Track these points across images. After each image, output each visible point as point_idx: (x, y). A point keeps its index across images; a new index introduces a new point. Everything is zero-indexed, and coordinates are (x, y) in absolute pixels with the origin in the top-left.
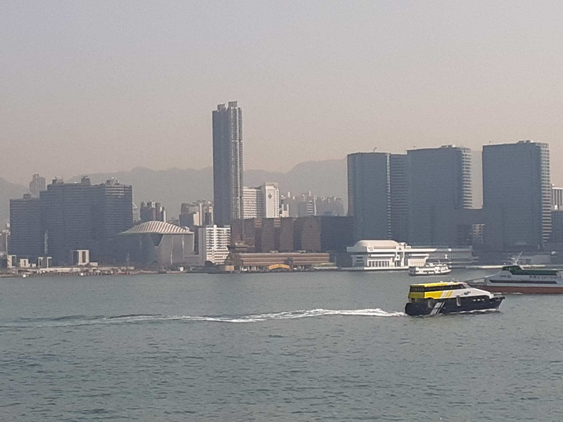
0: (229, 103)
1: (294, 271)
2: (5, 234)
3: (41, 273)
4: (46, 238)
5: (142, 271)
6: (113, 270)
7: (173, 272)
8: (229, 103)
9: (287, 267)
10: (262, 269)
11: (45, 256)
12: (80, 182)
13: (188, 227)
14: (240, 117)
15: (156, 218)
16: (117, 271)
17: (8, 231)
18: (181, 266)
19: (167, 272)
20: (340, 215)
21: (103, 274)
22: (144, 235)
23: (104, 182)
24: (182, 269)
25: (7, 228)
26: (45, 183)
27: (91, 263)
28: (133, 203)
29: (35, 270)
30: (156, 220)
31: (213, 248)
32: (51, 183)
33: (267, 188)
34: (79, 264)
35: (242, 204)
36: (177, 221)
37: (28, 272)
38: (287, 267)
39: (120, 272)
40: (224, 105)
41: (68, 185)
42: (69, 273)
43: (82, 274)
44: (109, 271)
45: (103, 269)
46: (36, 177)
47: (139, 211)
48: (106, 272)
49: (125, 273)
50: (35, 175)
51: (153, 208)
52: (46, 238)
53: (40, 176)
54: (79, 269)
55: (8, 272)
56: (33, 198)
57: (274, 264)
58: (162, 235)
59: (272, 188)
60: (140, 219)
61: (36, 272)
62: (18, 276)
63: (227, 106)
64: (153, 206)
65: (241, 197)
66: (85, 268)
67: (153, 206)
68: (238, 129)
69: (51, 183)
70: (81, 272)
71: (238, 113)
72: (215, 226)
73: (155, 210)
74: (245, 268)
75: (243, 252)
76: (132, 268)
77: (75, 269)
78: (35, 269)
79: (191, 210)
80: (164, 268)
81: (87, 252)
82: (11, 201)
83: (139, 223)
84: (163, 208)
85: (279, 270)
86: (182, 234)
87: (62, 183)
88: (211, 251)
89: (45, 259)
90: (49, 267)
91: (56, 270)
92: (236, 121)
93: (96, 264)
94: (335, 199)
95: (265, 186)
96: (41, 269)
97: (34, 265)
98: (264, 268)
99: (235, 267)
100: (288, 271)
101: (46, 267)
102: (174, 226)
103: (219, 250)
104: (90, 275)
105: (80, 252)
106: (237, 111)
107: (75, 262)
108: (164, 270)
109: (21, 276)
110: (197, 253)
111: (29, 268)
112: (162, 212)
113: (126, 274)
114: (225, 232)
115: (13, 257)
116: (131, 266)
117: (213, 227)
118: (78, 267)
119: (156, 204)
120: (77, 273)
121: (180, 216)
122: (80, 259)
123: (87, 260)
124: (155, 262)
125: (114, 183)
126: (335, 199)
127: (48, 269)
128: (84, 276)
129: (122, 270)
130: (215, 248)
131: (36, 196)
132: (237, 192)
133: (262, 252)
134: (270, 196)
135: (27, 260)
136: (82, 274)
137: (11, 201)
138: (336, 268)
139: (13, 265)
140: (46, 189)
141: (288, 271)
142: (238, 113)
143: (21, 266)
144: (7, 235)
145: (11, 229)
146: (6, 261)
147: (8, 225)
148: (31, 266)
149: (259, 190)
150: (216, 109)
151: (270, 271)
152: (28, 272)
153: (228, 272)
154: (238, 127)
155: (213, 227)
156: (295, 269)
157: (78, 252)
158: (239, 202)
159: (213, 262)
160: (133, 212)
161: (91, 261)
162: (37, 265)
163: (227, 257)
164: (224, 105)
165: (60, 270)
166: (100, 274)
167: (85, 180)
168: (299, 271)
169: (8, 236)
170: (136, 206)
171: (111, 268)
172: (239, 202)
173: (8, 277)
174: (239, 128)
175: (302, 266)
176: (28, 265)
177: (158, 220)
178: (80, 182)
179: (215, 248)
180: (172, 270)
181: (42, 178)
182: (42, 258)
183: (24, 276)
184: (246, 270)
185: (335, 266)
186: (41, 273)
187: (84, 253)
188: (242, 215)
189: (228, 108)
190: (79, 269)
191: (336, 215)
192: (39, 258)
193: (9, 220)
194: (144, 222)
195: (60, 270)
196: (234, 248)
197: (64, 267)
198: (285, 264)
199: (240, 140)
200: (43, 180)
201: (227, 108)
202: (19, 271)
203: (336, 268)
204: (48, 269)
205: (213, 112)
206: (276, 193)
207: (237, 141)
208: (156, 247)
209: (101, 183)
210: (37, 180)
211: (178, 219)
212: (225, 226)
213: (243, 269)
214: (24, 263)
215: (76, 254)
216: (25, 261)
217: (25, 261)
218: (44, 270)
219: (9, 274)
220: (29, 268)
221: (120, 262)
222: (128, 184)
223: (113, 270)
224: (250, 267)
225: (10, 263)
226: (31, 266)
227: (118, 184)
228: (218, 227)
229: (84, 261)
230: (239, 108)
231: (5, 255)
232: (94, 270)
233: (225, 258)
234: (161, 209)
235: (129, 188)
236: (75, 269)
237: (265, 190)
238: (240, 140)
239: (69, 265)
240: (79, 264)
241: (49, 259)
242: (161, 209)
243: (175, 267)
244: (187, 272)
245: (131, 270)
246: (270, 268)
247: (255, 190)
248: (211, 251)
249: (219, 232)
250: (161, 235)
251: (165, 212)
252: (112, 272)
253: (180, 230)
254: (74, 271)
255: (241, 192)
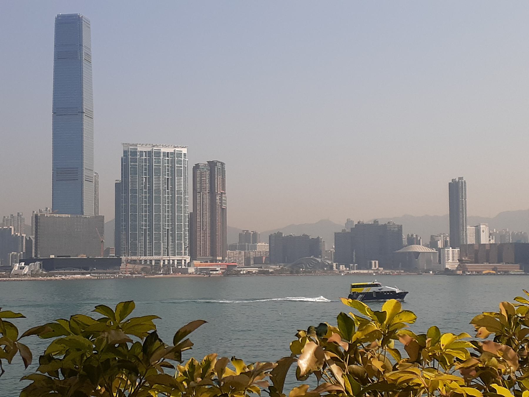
0: (459, 178)
1: (498, 275)
2: (332, 252)
3: (351, 273)
4: (354, 254)
5: (408, 273)
6: (392, 272)
7: (426, 274)
8: (459, 178)
9: (494, 272)
10: (479, 273)
11: (354, 264)
12: (373, 223)
13: (435, 248)
14: (465, 186)
15: (416, 243)
16: (394, 273)
17: (333, 249)
18: (431, 271)
19: (423, 274)
20: (526, 242)
21: (386, 274)
22: (410, 253)
23: (387, 223)
24: (431, 272)
25: (333, 248)
26: (353, 224)
27: (379, 268)
28: (403, 235)
29: (348, 272)
30: (416, 244)
31: (449, 260)
32: (357, 223)
33: (481, 226)
34: (373, 268)
35: (466, 236)
36: (428, 245)
37: (345, 272)
38: (494, 272)
39: (396, 273)
40: (456, 179)
41: (366, 225)
42: (368, 274)
43: (374, 274)
44: (390, 273)
45: (386, 271)
46: (349, 220)
47: (406, 239)
48: (388, 273)
49: (399, 274)
50: (348, 219)
51: (414, 238)
52: (354, 254)
53: (351, 220)
54: (372, 272)
55: (334, 272)
56: (347, 232)
57: (486, 270)
58: (420, 253)
59: (484, 226)
60: (407, 243)
61: (349, 273)
62: (339, 275)
63: (457, 180)
64: (414, 236)
65: (466, 231)
66: (376, 271)
67: (414, 236)
68: (464, 193)
69: (357, 223)
70: (374, 273)
71: (464, 184)
72: (451, 248)
73: (415, 239)
74: (468, 272)
75: (467, 263)
76: (403, 271)
77: (370, 271)
78: (348, 271)
79: (436, 239)
80: (421, 272)
81: (377, 262)
82: (335, 233)
83: (406, 246)
84: (420, 238)
85: (489, 274)
86: (431, 252)
87: (363, 223)
88: (448, 262)
89: (354, 266)
90: (356, 270)
91: (360, 272)
92: (463, 189)
93: (382, 269)
94: (523, 233)
95: (480, 225)
96: (352, 271)
97: (348, 269)
98: (480, 273)
99: (463, 272)
100: (494, 274)
101: (354, 270)
102: (424, 247)
103: (453, 262)
104: (379, 274)
105: (373, 262)
106: (463, 182)
107: (370, 268)
108: (421, 273)
109: (341, 275)
110: (440, 263)
111: (345, 270)
112: (420, 240)
113: (399, 274)
114: (457, 251)
115: (336, 264)
116: (402, 270)
117: (449, 248)
118: (372, 270)
119: (416, 235)
120: (371, 274)
121: (430, 242)
122: (373, 266)
123: (377, 267)
124: (416, 268)
125: (392, 223)
126: (523, 233)
127: (356, 271)
128: (375, 275)
129: (397, 272)
130: (450, 261)
131: (348, 230)
132: (463, 229)
133: (479, 263)
134: (483, 231)
135: (344, 266)
136: (374, 274)
137: (335, 233)
138: (524, 273)
139: (336, 268)
140: (354, 227)
141: (494, 274)
142: (464, 184)
143: (341, 269)
144: (333, 252)
145: (335, 249)
146: (333, 266)
147: (334, 247)
148: (346, 269)
149: (476, 228)
150: (451, 181)
151: (484, 274)
152: (345, 272)
153: (459, 275)
154: (464, 192)
155: (449, 248)
156: (499, 273)
157: (372, 262)
158: (465, 234)
159: (450, 269)
160: (403, 240)
161: (379, 267)
162: (349, 268)
163: (458, 266)
164: (456, 179)
165: (362, 271)
166: (384, 274)
167: (376, 222)
168: (501, 274)
169: (334, 253)
170: (404, 236)
171: (390, 271)
172: (465, 234)
173: (334, 275)
174: (465, 192)
175: (503, 272)
176: (344, 269)
177: (417, 245)
178: (373, 223)
179: (450, 261)
180: (425, 273)
181: (352, 221)
182: (352, 265)
183: (343, 274)
184: (469, 273)
185: (523, 272)
186: (351, 273)
187: (375, 263)
188: (466, 241)
189: (458, 181)
190: (372, 272)
191: (523, 242)
192: (351, 265)
193: (334, 244)
194: (410, 245)
195: (362, 271)
196: (463, 261)
197: (364, 269)
198: (492, 270)
199: (465, 199)
200: (352, 222)
201: (457, 181)
202: (339, 272)
203: (524, 273)
204: (356, 271)
205: (449, 183)
206: (487, 229)
207: (464, 200)
208: (417, 260)
209: (385, 223)
210: (349, 222)
211: (429, 243)
212: (456, 248)
213: (467, 273)
214: (342, 267)
215: (371, 263)
216: (343, 266)
217: (343, 266)
218: (353, 271)
219: (334, 273)
220: (345, 270)
221: (395, 268)
222: (400, 224)
223: (392, 272)
224: (472, 272)
225: (335, 267)
226: (346, 269)
227: (394, 224)
228: (452, 248)
229: (375, 267)
230: (465, 181)
231: (332, 263)
232: (381, 272)
233: (457, 266)
234: (419, 238)
235: (400, 226)
236: (370, 271)
237: (480, 228)
238: (465, 199)
239: (367, 269)
240: (373, 268)
241: (356, 266)
242: (419, 238)
243: (427, 271)
244: (434, 274)
245: (402, 272)
246: (484, 272)
247: (474, 228)
248: (448, 262)
249: (453, 252)
250: (419, 253)
251: (421, 240)
252: (391, 273)
253: (430, 250)
254: (370, 272)
255: (466, 228)
